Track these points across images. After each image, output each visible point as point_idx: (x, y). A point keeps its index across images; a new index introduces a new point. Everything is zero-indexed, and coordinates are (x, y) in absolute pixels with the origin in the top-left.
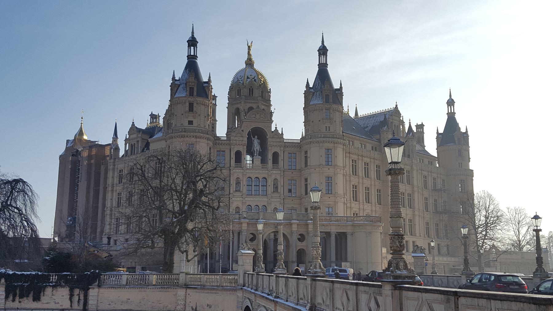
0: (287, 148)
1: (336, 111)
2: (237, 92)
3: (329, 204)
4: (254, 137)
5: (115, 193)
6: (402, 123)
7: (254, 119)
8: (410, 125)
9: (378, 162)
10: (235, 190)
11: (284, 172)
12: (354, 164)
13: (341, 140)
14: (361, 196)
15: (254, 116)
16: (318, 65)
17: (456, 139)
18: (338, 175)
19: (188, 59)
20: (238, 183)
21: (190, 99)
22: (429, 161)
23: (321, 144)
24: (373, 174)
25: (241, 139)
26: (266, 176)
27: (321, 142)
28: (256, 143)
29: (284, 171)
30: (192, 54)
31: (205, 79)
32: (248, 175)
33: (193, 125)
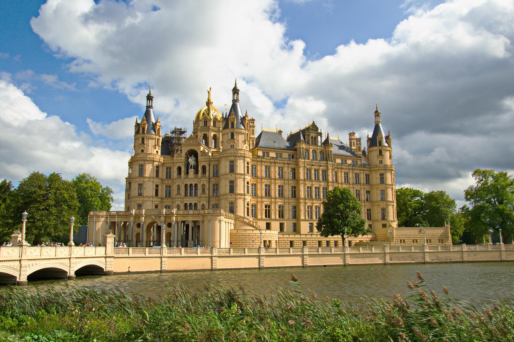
0: (212, 163)
3: (231, 201)
4: (191, 156)
6: (320, 134)
7: (189, 144)
9: (292, 166)
10: (176, 194)
11: (210, 180)
14: (275, 191)
15: (189, 142)
16: (232, 101)
17: (378, 142)
20: (179, 188)
21: (142, 136)
25: (180, 158)
26: (197, 182)
27: (226, 157)
29: (209, 179)
30: (148, 105)
32: (185, 183)
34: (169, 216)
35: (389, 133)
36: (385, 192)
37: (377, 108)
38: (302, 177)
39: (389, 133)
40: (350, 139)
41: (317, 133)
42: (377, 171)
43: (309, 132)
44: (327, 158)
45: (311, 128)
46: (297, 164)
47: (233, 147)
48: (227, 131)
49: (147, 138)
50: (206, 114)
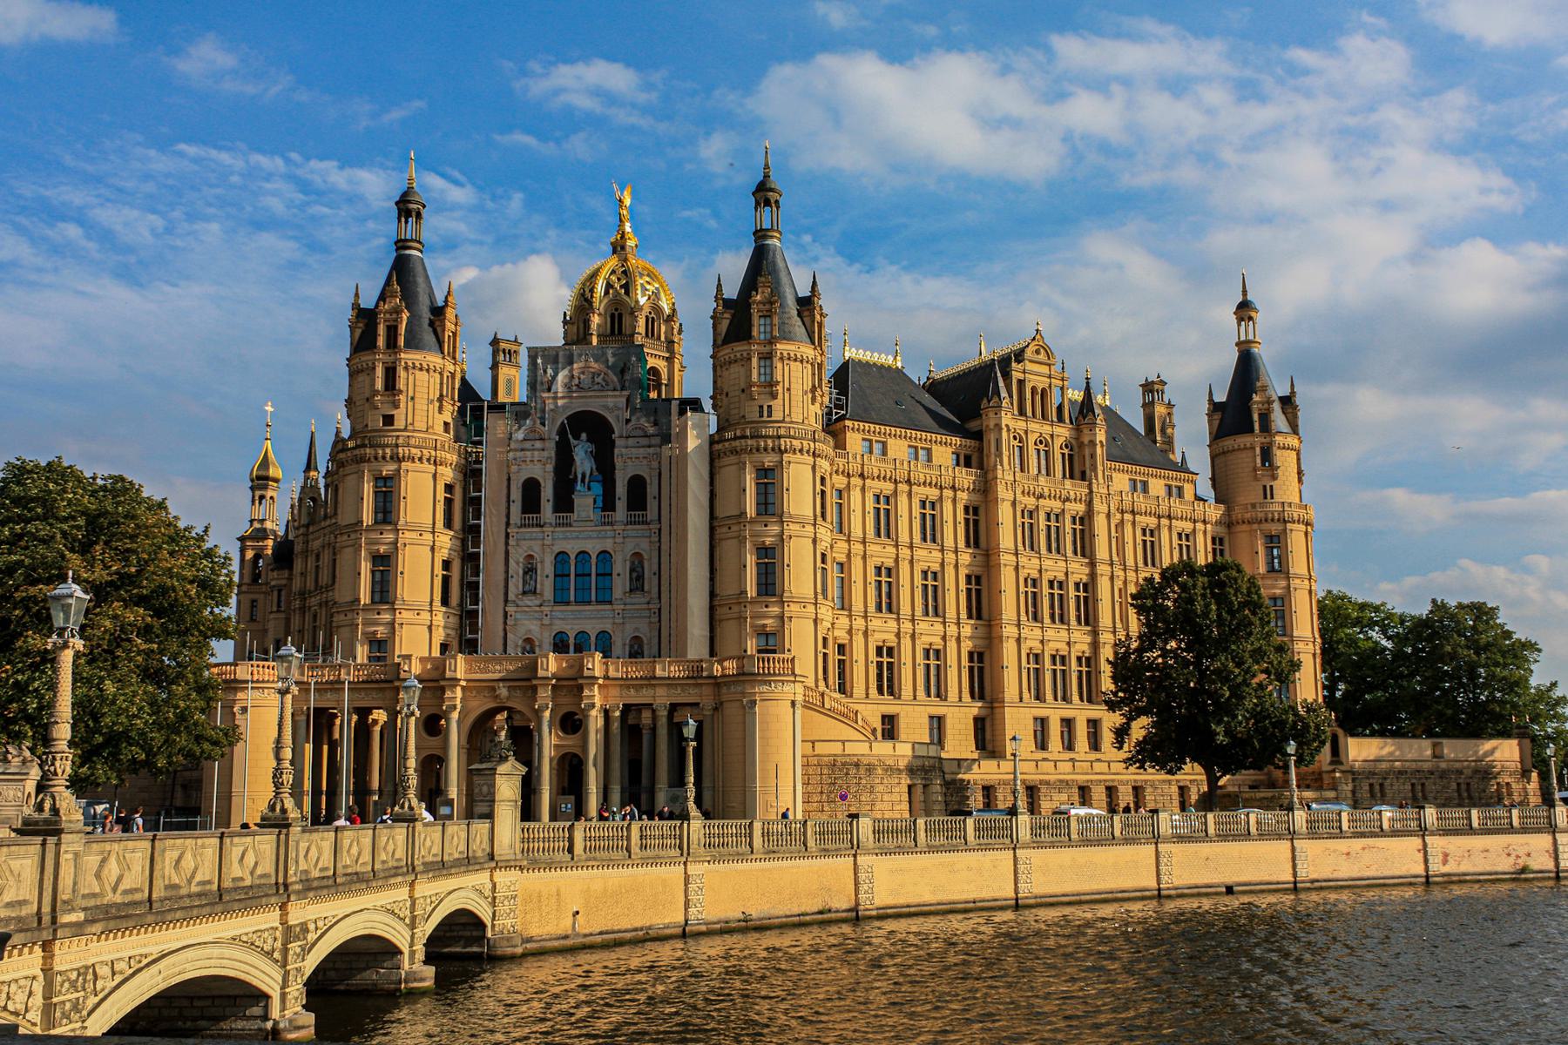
1: (789, 359)
2: (582, 326)
3: (765, 626)
5: (307, 614)
8: (1088, 383)
12: (882, 506)
13: (805, 443)
17: (1256, 417)
18: (793, 538)
19: (397, 250)
22: (1169, 487)
23: (747, 458)
24: (953, 529)
27: (744, 451)
28: (583, 460)
31: (440, 303)
33: (392, 425)
34: (573, 684)
35: (1292, 385)
36: (1286, 603)
37: (1245, 292)
38: (1006, 538)
39: (1292, 385)
40: (1148, 406)
41: (1050, 377)
42: (1255, 526)
43: (1024, 372)
44: (1088, 472)
45: (1029, 353)
46: (985, 488)
47: (770, 415)
48: (739, 348)
49: (406, 368)
50: (617, 286)
